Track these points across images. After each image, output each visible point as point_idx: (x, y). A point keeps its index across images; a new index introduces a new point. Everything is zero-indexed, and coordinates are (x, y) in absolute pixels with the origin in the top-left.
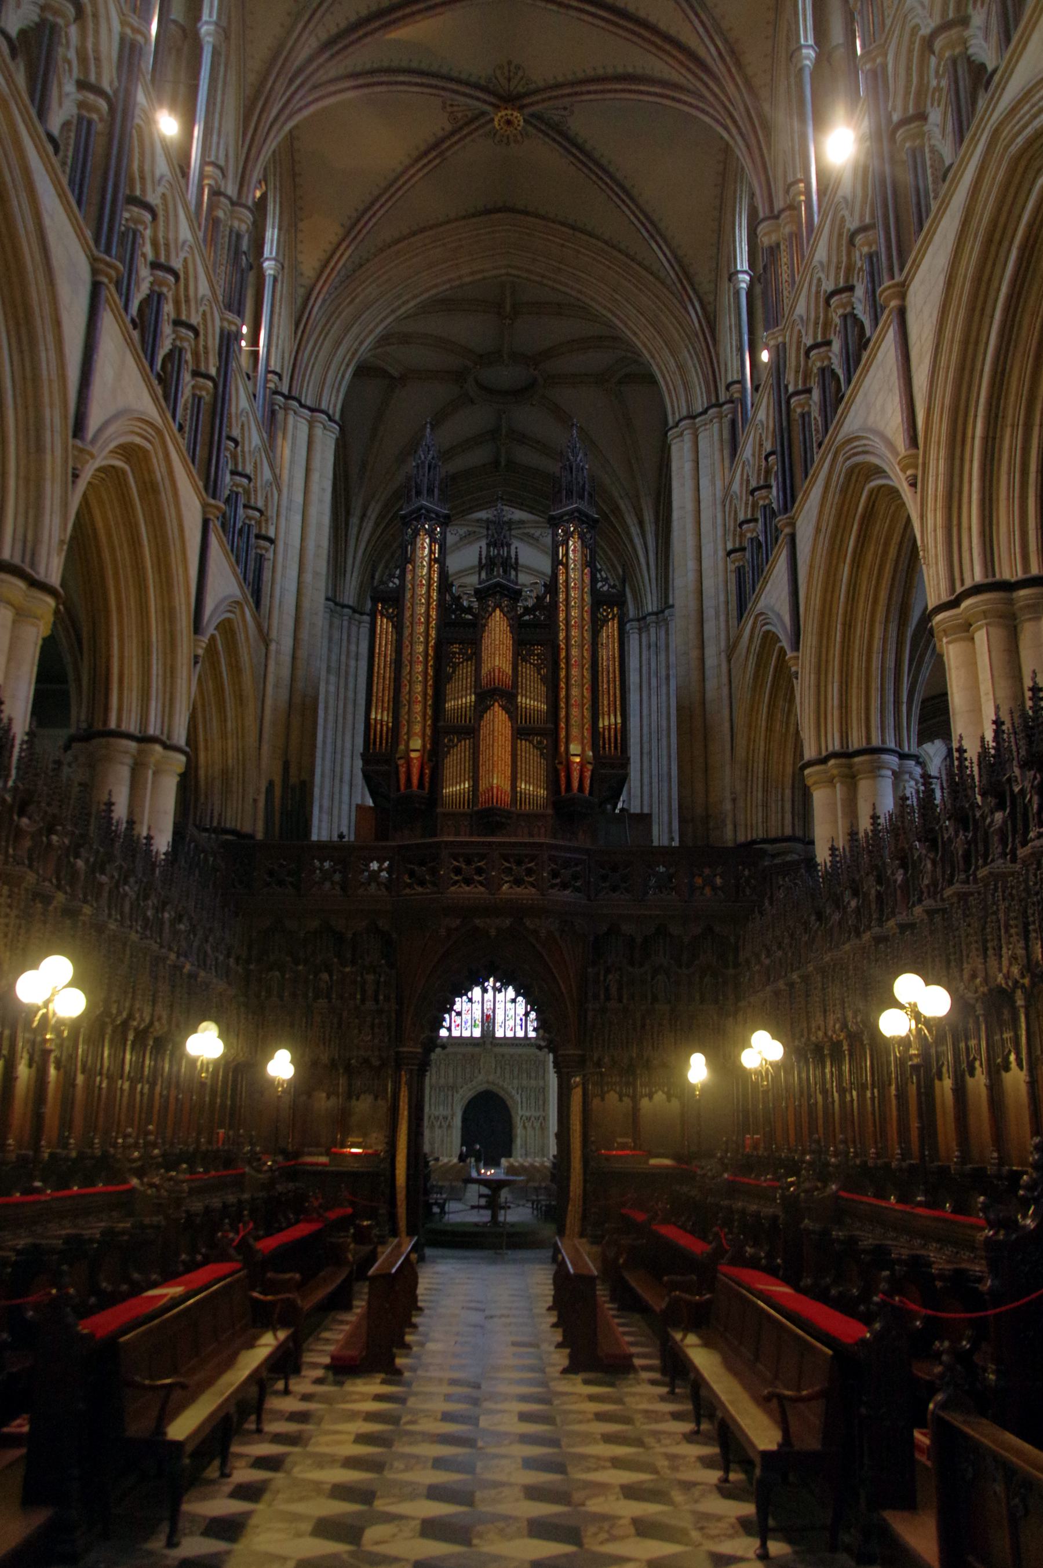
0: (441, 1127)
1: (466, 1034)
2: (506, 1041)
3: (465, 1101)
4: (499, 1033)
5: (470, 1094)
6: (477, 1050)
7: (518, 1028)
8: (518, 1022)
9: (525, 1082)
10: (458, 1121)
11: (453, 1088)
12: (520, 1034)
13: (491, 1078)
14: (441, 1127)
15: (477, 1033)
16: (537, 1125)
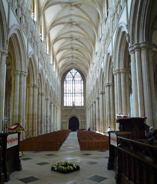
0: (64, 124)
1: (69, 105)
2: (77, 107)
3: (69, 119)
4: (76, 105)
5: (71, 117)
6: (72, 108)
7: (80, 104)
8: (80, 103)
9: (81, 114)
10: (68, 122)
11: (67, 116)
12: (80, 105)
13: (75, 114)
14: (64, 124)
15: (72, 105)
16: (84, 123)
